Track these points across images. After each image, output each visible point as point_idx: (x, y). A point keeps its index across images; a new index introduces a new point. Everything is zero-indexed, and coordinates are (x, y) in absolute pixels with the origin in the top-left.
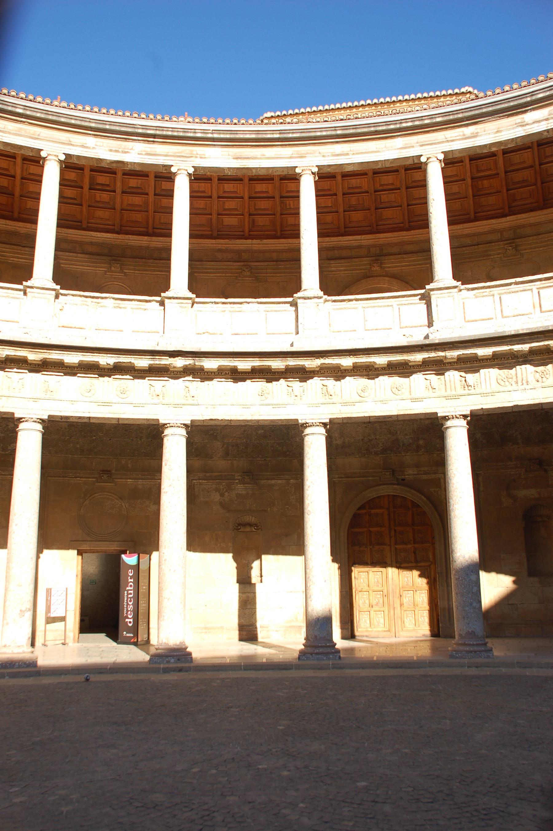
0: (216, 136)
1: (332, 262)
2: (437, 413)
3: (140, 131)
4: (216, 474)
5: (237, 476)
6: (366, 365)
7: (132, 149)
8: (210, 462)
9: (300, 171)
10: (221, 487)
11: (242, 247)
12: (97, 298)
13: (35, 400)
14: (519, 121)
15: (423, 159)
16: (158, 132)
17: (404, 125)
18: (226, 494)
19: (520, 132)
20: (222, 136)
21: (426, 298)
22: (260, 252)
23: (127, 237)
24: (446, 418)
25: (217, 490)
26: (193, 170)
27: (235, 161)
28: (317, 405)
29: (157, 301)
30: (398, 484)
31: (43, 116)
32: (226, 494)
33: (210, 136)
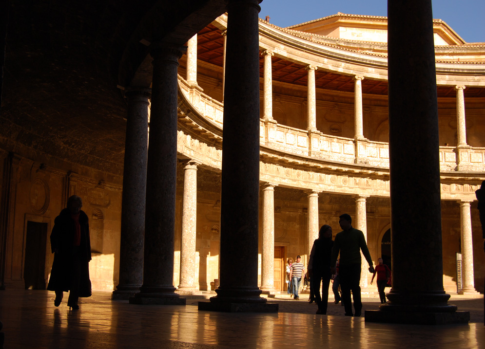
0: (374, 63)
1: (377, 107)
3: (346, 58)
5: (334, 213)
8: (323, 205)
11: (335, 94)
13: (317, 184)
15: (457, 87)
16: (352, 59)
17: (451, 71)
20: (377, 64)
21: (456, 151)
22: (342, 97)
23: (284, 83)
29: (352, 141)
31: (312, 49)
33: (372, 63)
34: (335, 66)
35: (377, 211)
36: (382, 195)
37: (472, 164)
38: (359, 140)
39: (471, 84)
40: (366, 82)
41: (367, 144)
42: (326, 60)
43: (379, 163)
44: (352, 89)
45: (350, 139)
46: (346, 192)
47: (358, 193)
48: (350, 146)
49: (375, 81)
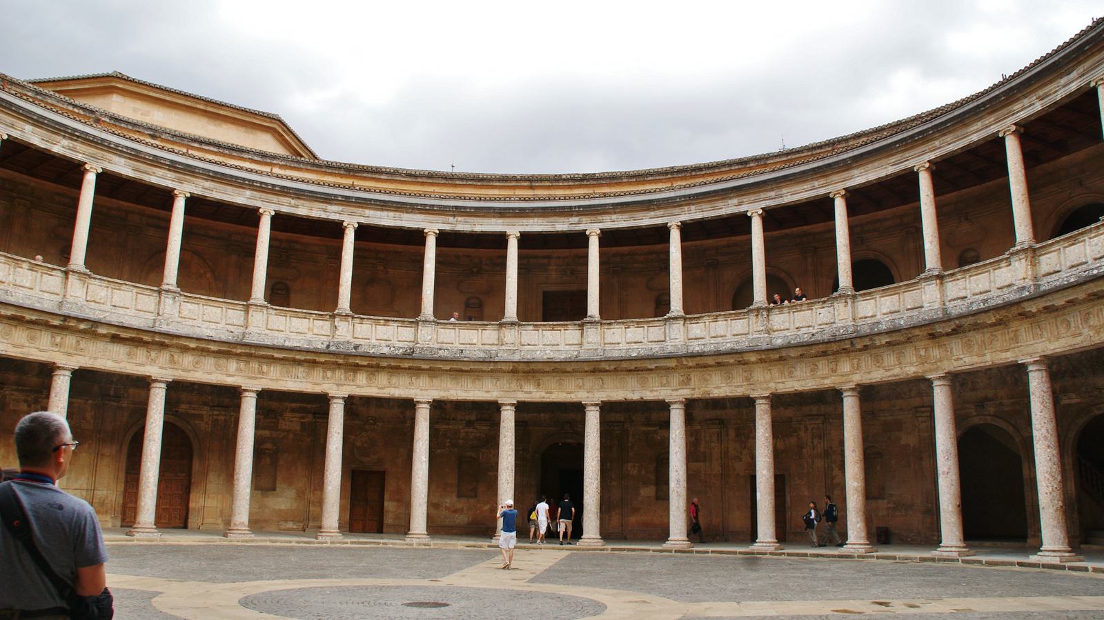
0: (124, 150)
2: (241, 386)
4: (27, 388)
6: (203, 347)
7: (59, 142)
8: (24, 377)
9: (177, 193)
10: (30, 399)
12: (18, 260)
14: (324, 207)
15: (261, 211)
18: (33, 406)
19: (323, 215)
24: (246, 390)
25: (25, 401)
26: (101, 170)
27: (133, 171)
28: (166, 368)
30: (172, 415)
32: (33, 406)
34: (47, 141)
35: (125, 394)
36: (103, 368)
37: (268, 331)
38: (73, 272)
39: (285, 209)
40: (106, 181)
41: (88, 280)
42: (28, 128)
43: (108, 314)
44: (78, 185)
45: (56, 267)
46: (31, 357)
47: (55, 361)
48: (53, 280)
49: (146, 185)
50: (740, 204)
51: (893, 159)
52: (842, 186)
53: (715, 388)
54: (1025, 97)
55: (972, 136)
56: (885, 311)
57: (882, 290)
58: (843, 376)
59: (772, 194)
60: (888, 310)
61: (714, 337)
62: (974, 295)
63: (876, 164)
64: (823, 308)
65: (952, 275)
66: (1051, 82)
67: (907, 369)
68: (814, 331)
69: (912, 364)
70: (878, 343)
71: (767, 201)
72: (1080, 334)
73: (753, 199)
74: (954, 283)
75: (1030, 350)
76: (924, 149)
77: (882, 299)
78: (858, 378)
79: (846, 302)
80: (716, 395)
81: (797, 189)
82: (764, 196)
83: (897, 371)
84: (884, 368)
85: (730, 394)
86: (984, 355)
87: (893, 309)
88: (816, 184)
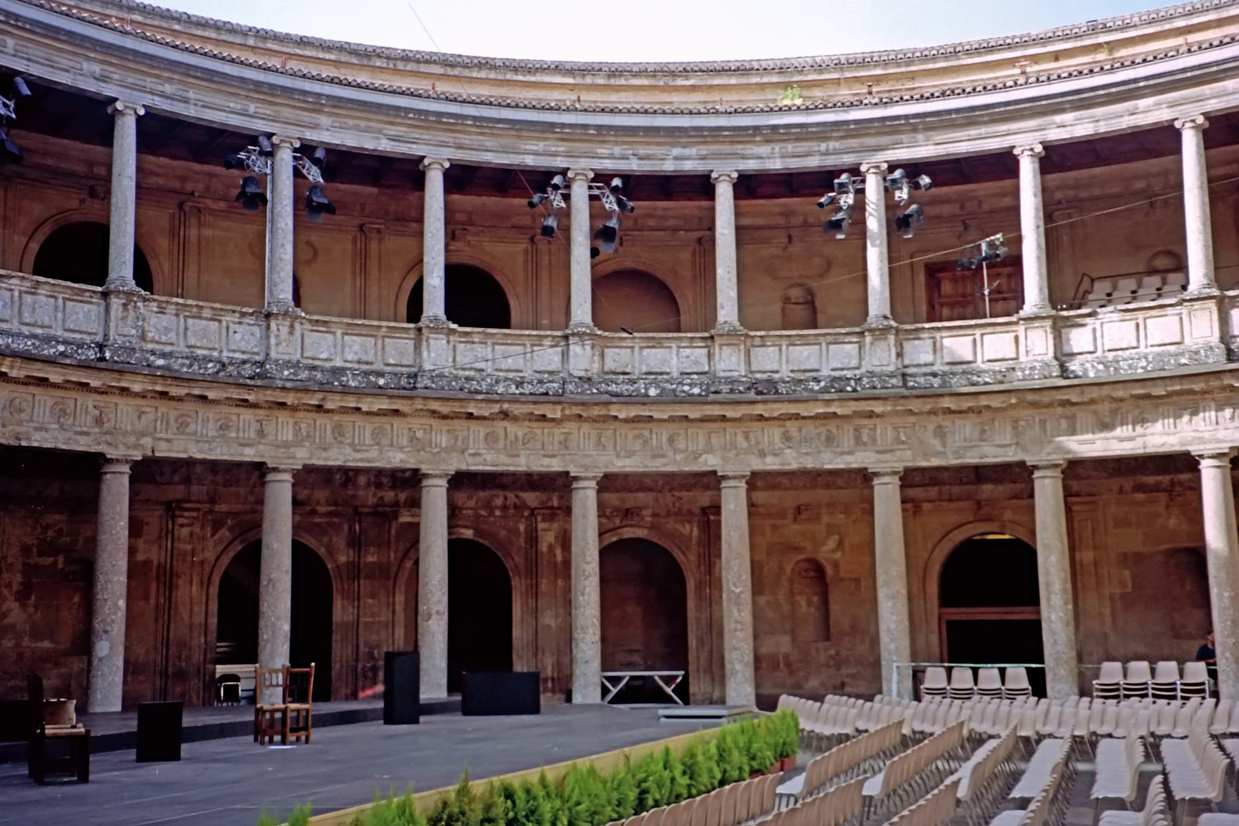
50: (103, 79)
51: (393, 131)
52: (295, 132)
53: (36, 429)
54: (616, 143)
55: (526, 156)
56: (350, 358)
57: (349, 324)
58: (278, 447)
59: (168, 88)
60: (356, 358)
61: (27, 324)
62: (496, 370)
63: (363, 124)
64: (240, 323)
65: (466, 334)
66: (658, 144)
67: (391, 454)
68: (225, 360)
69: (401, 449)
70: (365, 408)
71: (156, 98)
72: (663, 456)
73: (130, 80)
74: (469, 346)
75: (587, 461)
76: (445, 139)
77: (346, 338)
78: (303, 456)
79: (292, 326)
80: (35, 444)
81: (217, 101)
82: (153, 86)
83: (373, 453)
84: (352, 445)
85: (64, 447)
86: (518, 456)
87: (364, 358)
88: (252, 108)
